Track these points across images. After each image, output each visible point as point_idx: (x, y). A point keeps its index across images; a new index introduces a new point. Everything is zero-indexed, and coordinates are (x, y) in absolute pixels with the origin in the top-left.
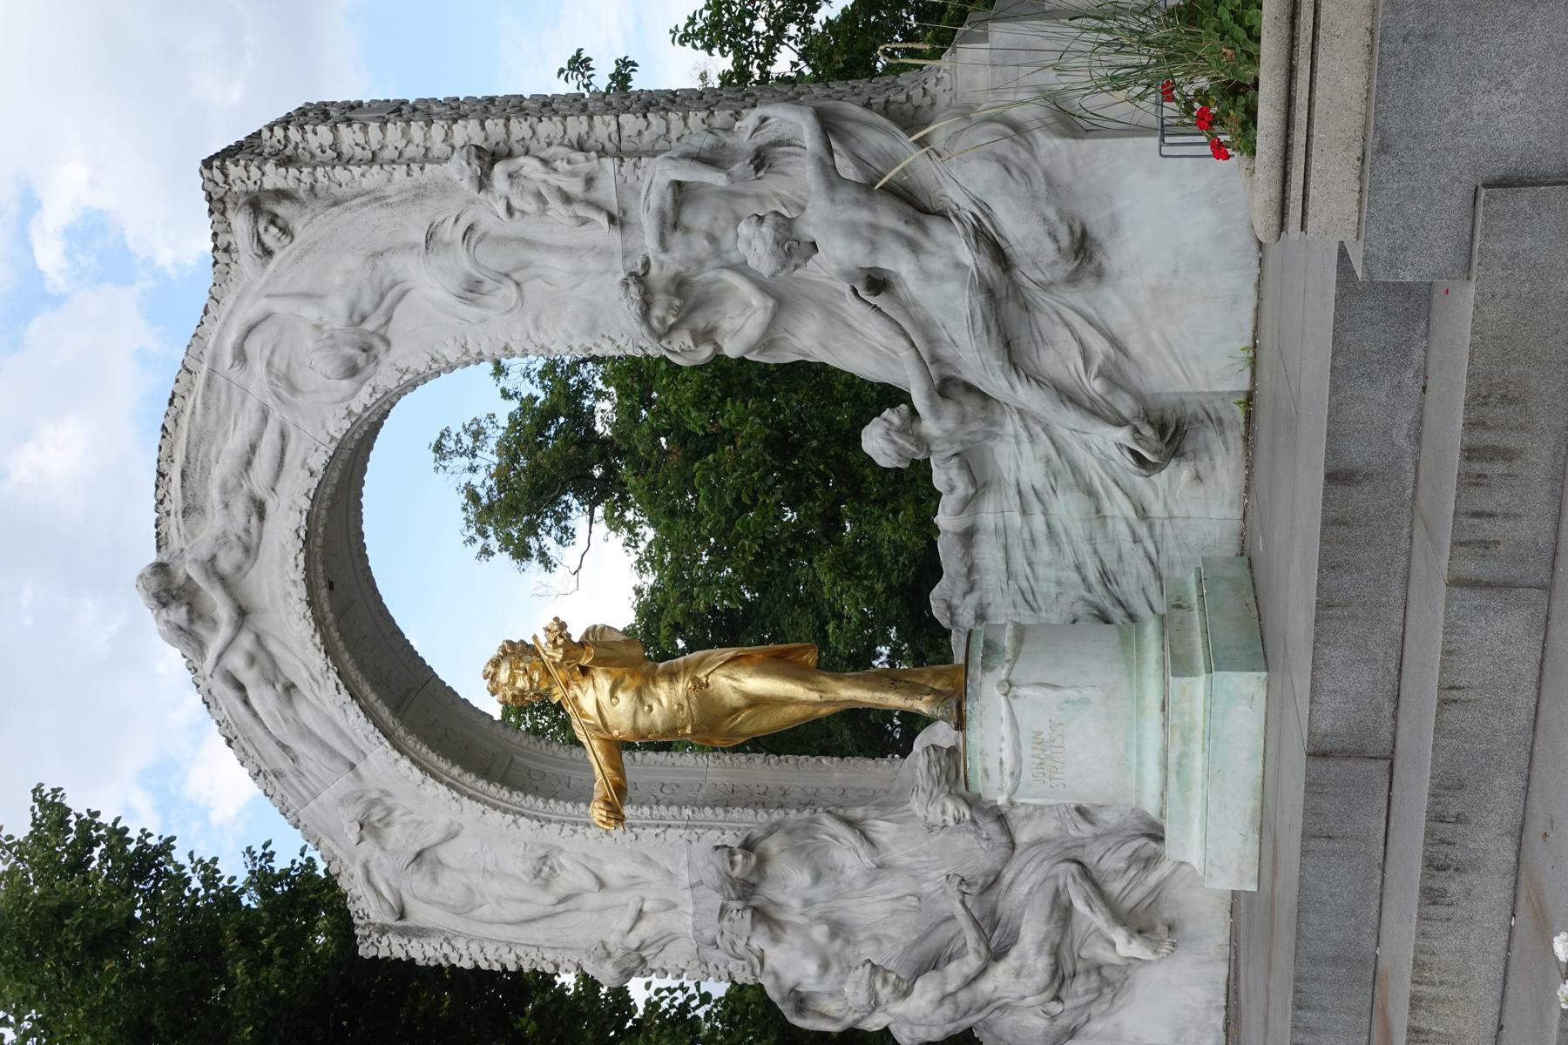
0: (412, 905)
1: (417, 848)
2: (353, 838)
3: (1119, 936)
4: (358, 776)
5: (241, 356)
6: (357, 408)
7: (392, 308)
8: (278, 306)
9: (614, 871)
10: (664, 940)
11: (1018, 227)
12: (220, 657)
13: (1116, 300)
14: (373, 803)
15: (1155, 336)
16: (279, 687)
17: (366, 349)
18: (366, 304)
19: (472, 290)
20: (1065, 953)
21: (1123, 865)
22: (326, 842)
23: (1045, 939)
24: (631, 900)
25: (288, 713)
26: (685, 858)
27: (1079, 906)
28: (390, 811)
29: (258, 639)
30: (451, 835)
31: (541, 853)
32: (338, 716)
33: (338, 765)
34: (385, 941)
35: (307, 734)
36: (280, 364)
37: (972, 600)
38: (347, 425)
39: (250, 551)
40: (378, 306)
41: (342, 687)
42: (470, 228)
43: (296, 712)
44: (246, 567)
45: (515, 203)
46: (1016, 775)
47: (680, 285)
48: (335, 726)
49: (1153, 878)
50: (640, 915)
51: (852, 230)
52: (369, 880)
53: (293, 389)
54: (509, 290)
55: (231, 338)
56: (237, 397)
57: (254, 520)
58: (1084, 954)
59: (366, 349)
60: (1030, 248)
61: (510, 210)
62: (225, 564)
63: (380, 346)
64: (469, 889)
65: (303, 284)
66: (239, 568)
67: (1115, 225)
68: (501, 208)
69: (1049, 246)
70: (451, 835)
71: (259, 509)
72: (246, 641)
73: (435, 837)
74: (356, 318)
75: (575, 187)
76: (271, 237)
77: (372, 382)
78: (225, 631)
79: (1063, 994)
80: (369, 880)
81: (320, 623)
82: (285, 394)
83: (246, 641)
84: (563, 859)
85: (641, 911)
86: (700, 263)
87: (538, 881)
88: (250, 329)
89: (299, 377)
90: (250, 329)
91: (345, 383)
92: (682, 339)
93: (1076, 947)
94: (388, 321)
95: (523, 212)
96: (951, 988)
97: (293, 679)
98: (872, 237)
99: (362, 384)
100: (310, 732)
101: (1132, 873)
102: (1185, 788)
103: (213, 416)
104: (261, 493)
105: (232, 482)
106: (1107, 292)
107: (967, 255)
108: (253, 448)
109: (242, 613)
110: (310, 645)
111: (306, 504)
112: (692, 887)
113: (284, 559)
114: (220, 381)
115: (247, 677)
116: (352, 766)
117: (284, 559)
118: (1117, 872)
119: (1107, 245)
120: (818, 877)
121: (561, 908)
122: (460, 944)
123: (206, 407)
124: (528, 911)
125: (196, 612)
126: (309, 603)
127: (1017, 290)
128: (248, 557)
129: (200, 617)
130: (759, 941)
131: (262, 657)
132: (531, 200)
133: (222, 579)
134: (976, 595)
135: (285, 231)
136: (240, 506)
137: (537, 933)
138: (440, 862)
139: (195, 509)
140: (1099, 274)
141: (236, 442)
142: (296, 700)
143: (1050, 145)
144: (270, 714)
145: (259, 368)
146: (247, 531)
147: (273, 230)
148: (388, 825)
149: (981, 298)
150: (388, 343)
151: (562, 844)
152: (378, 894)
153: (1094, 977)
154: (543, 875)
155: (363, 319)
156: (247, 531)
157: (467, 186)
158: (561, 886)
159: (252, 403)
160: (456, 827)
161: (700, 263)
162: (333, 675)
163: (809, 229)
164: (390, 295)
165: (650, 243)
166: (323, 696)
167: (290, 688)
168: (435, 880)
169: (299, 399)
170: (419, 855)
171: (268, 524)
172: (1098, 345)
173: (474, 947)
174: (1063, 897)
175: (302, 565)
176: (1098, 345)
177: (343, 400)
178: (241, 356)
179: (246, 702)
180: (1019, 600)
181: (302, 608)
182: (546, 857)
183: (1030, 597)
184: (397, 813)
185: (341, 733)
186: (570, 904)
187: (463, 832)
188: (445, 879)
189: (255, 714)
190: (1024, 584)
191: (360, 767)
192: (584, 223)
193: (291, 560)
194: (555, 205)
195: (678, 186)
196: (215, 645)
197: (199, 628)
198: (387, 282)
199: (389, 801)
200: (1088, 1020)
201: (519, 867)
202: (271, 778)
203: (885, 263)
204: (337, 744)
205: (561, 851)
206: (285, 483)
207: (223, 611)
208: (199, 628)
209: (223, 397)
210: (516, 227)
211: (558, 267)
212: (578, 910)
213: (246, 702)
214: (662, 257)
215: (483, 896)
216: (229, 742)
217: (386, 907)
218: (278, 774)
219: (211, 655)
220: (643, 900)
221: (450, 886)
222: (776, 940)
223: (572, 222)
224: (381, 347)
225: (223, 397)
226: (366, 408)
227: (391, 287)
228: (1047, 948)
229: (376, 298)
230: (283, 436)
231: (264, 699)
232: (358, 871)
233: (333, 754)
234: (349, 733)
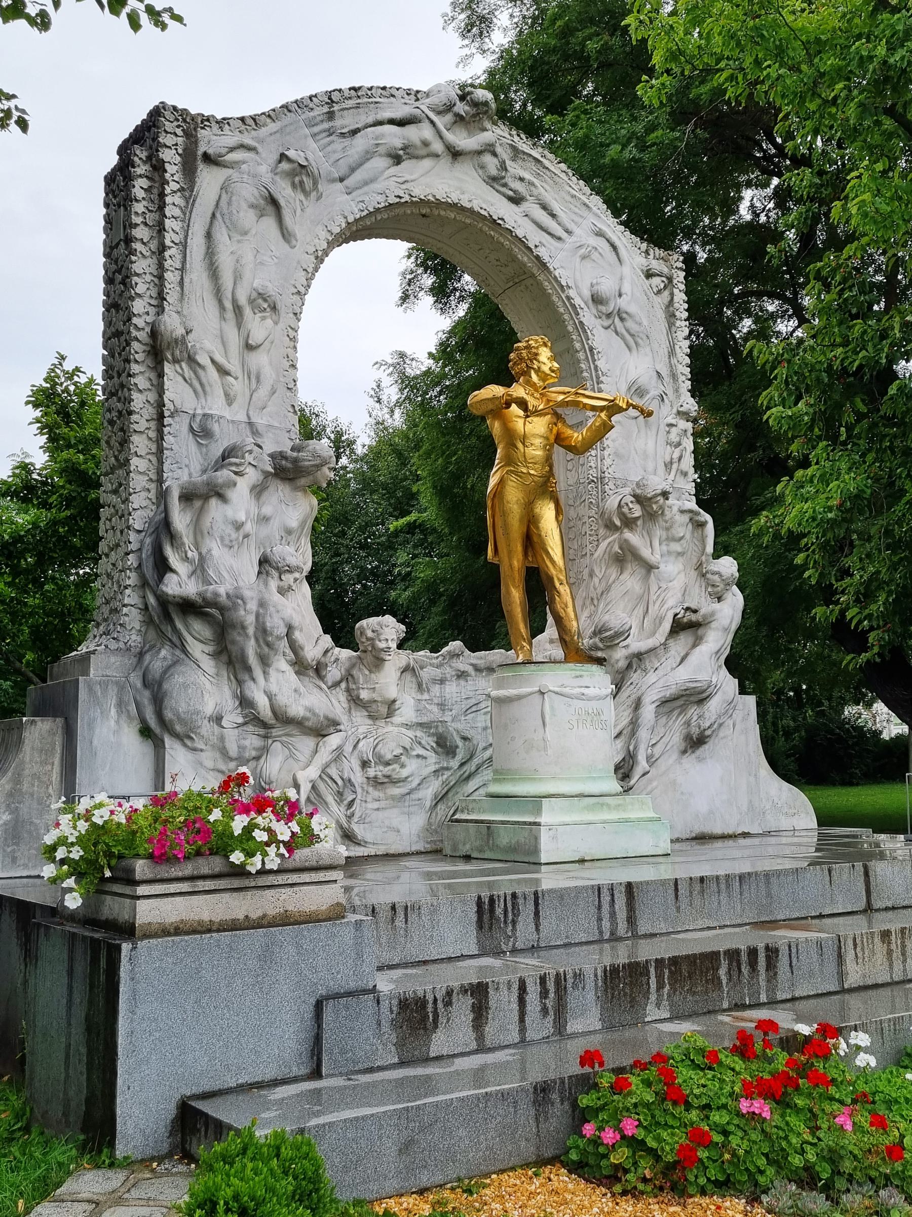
1: (282, 202)
2: (291, 153)
3: (313, 772)
4: (333, 181)
5: (600, 234)
6: (572, 293)
7: (623, 338)
8: (626, 270)
9: (260, 360)
10: (201, 389)
12: (432, 122)
13: (671, 761)
14: (315, 183)
15: (655, 784)
16: (401, 152)
17: (609, 316)
18: (630, 324)
20: (289, 729)
21: (346, 776)
22: (272, 127)
23: (314, 714)
24: (233, 366)
25: (382, 150)
26: (276, 424)
28: (306, 194)
29: (437, 156)
30: (286, 235)
31: (278, 306)
32: (378, 186)
33: (343, 169)
34: (179, 131)
35: (367, 156)
36: (595, 256)
37: (470, 669)
38: (564, 284)
39: (494, 181)
40: (627, 331)
41: (398, 200)
42: (663, 400)
43: (380, 155)
44: (480, 172)
45: (674, 429)
46: (582, 697)
48: (372, 181)
49: (330, 799)
50: (223, 372)
52: (242, 146)
53: (584, 258)
55: (610, 234)
56: (576, 219)
57: (511, 193)
58: (277, 745)
59: (609, 316)
60: (707, 715)
61: (671, 425)
63: (607, 323)
64: (246, 233)
66: (482, 167)
67: (700, 760)
68: (670, 420)
69: (707, 725)
70: (286, 235)
71: (516, 200)
72: (438, 147)
74: (624, 315)
77: (586, 309)
78: (450, 137)
79: (250, 728)
80: (242, 146)
81: (439, 204)
82: (583, 251)
84: (269, 322)
85: (227, 373)
86: (667, 529)
87: (254, 295)
88: (614, 248)
89: (588, 264)
90: (614, 248)
91: (587, 294)
92: (637, 511)
93: (284, 738)
94: (617, 333)
95: (668, 432)
96: (297, 635)
97: (404, 165)
99: (586, 303)
100: (368, 159)
101: (340, 782)
102: (590, 808)
103: (568, 198)
104: (525, 206)
105: (535, 192)
106: (675, 756)
108: (553, 216)
109: (455, 154)
110: (428, 191)
111: (520, 233)
112: (250, 424)
113: (484, 201)
114: (585, 213)
115: (413, 133)
116: (341, 180)
117: (484, 201)
118: (342, 771)
119: (693, 756)
120: (289, 532)
121: (228, 305)
123: (573, 196)
125: (459, 119)
126: (455, 205)
128: (489, 177)
129: (455, 122)
130: (252, 476)
131: (423, 152)
132: (678, 439)
133: (479, 153)
134: (473, 673)
135: (659, 292)
137: (197, 275)
138: (262, 216)
139: (515, 156)
140: (684, 752)
141: (556, 207)
142: (389, 161)
144: (382, 136)
145: (594, 241)
146: (505, 185)
147: (662, 286)
148: (294, 186)
149: (703, 685)
150: (606, 328)
151: (281, 325)
152: (232, 150)
153: (254, 754)
154: (260, 301)
155: (622, 319)
156: (505, 185)
158: (247, 311)
160: (294, 242)
161: (667, 529)
162: (407, 198)
164: (633, 341)
166: (391, 183)
167: (397, 160)
168: (252, 206)
169: (578, 260)
170: (273, 202)
171: (505, 200)
173: (177, 212)
174: (332, 730)
175: (483, 212)
177: (577, 287)
178: (600, 234)
179: (392, 122)
180: (473, 701)
181: (454, 198)
182: (274, 308)
183: (474, 709)
184: (302, 197)
185: (366, 183)
186: (230, 315)
187: (286, 246)
188: (251, 215)
189: (380, 123)
190: (483, 705)
191: (339, 185)
192: (666, 465)
193: (484, 206)
195: (702, 525)
197: (449, 117)
198: (640, 341)
199: (314, 194)
200: (195, 749)
202: (326, 109)
204: (358, 176)
205: (276, 323)
208: (449, 117)
209: (577, 210)
210: (663, 428)
212: (223, 318)
213: (392, 122)
214: (675, 509)
215: (239, 241)
216: (355, 89)
217: (224, 151)
218: (331, 115)
219: (432, 115)
220: (236, 378)
221: (247, 217)
222: (253, 488)
223: (668, 459)
224: (606, 323)
225: (577, 210)
226: (569, 298)
227: (636, 343)
228: (308, 715)
229: (632, 332)
230: (559, 239)
231: (394, 136)
232: (247, 140)
233: (353, 170)
234: (366, 189)
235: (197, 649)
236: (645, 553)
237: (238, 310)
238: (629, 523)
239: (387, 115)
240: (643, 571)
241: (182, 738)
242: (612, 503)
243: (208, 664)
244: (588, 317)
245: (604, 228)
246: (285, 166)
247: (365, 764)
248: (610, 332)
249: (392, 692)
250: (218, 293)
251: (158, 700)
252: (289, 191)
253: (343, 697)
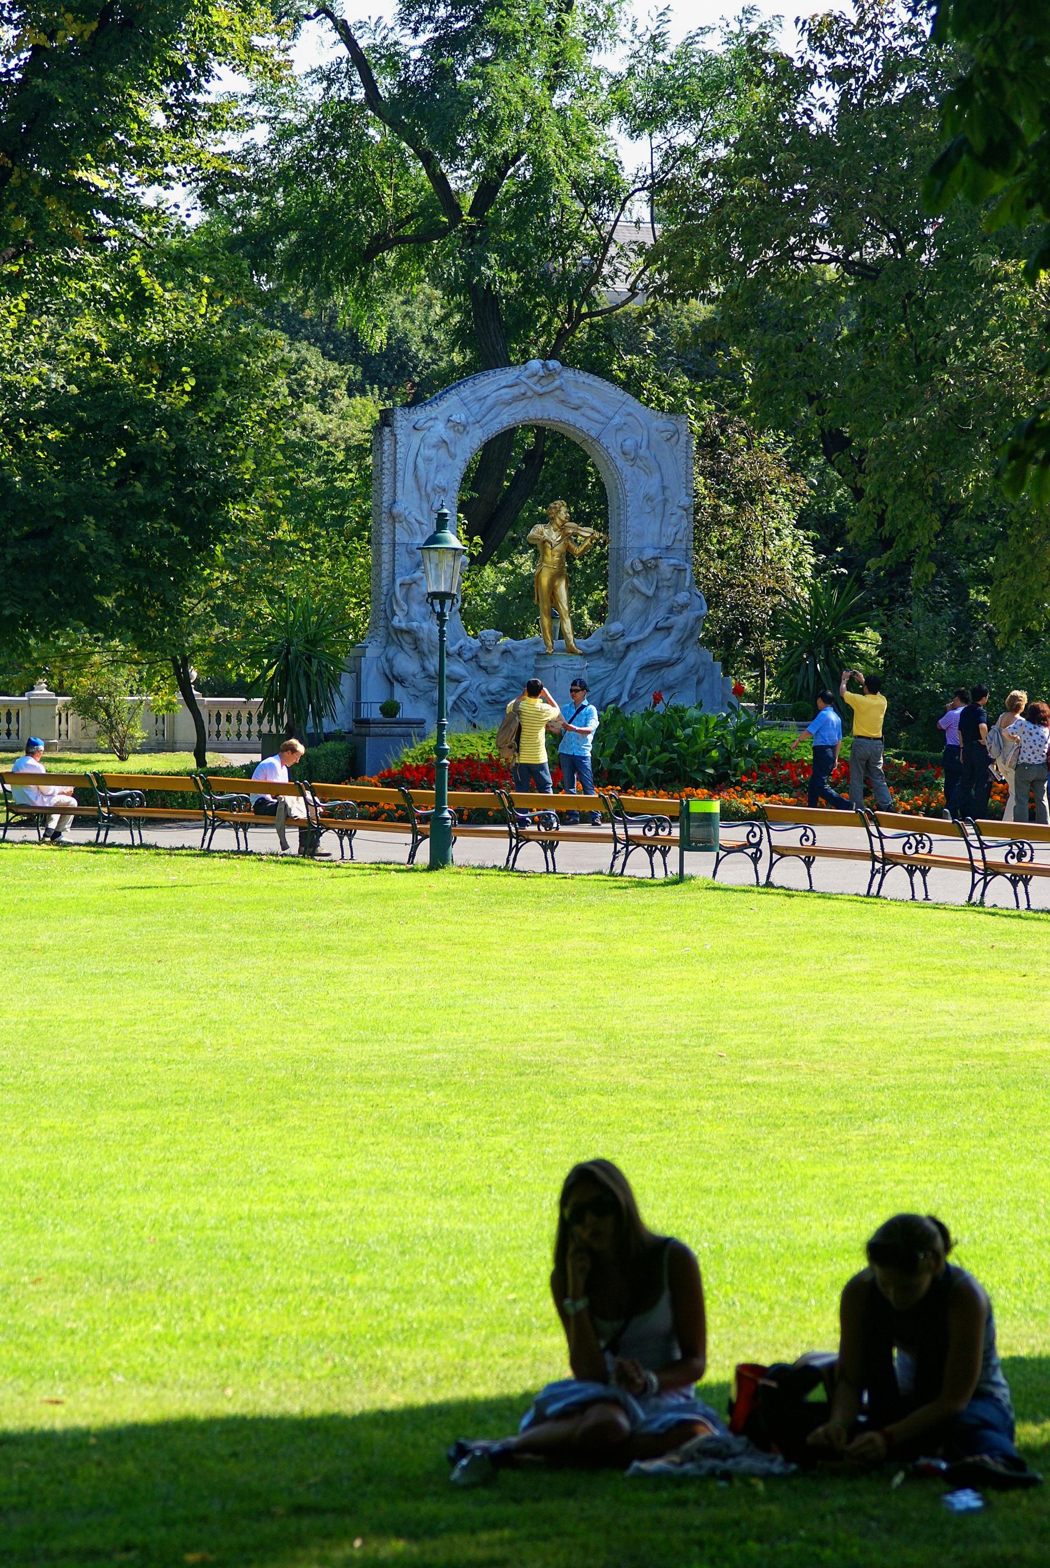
0: (421, 434)
5: (629, 414)
11: (679, 669)
14: (465, 427)
19: (649, 498)
27: (464, 684)
30: (453, 456)
47: (656, 566)
51: (686, 625)
54: (648, 510)
62: (558, 392)
65: (652, 443)
70: (453, 456)
73: (452, 450)
75: (679, 537)
76: (667, 435)
83: (529, 393)
98: (684, 630)
107: (676, 656)
115: (516, 391)
122: (403, 450)
124: (423, 480)
127: (660, 669)
136: (578, 402)
143: (695, 678)
157: (682, 504)
159: (611, 414)
163: (685, 613)
165: (672, 561)
172: (642, 692)
176: (642, 692)
178: (629, 414)
194: (675, 530)
196: (530, 382)
197: (536, 378)
201: (441, 479)
203: (674, 633)
204: (487, 418)
206: (584, 420)
207: (538, 388)
208: (536, 378)
211: (655, 528)
221: (430, 453)
235: (406, 647)
236: (644, 589)
237: (428, 495)
238: (637, 573)
239: (504, 384)
240: (643, 598)
241: (401, 682)
242: (628, 563)
243: (411, 653)
244: (620, 462)
245: (631, 410)
246: (450, 424)
247: (483, 694)
248: (635, 468)
249: (496, 663)
250: (419, 489)
251: (391, 667)
252: (452, 435)
253: (473, 664)
